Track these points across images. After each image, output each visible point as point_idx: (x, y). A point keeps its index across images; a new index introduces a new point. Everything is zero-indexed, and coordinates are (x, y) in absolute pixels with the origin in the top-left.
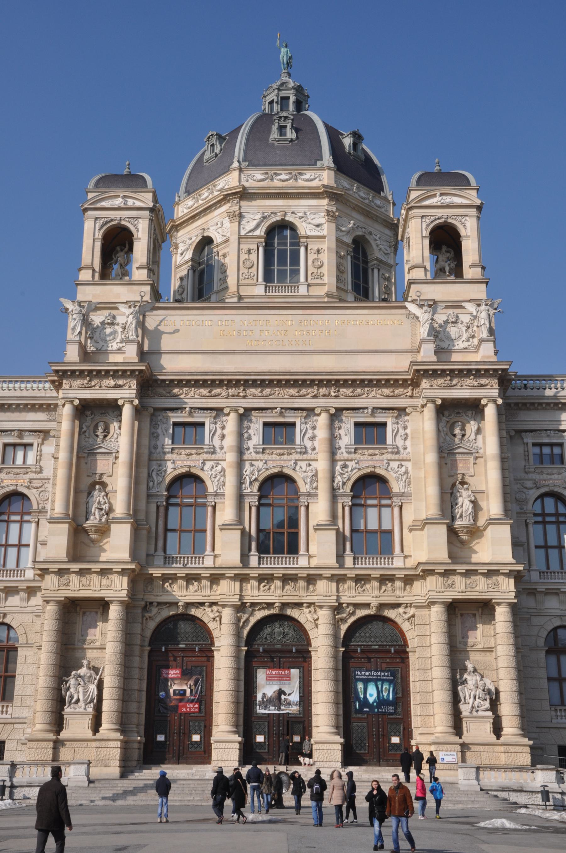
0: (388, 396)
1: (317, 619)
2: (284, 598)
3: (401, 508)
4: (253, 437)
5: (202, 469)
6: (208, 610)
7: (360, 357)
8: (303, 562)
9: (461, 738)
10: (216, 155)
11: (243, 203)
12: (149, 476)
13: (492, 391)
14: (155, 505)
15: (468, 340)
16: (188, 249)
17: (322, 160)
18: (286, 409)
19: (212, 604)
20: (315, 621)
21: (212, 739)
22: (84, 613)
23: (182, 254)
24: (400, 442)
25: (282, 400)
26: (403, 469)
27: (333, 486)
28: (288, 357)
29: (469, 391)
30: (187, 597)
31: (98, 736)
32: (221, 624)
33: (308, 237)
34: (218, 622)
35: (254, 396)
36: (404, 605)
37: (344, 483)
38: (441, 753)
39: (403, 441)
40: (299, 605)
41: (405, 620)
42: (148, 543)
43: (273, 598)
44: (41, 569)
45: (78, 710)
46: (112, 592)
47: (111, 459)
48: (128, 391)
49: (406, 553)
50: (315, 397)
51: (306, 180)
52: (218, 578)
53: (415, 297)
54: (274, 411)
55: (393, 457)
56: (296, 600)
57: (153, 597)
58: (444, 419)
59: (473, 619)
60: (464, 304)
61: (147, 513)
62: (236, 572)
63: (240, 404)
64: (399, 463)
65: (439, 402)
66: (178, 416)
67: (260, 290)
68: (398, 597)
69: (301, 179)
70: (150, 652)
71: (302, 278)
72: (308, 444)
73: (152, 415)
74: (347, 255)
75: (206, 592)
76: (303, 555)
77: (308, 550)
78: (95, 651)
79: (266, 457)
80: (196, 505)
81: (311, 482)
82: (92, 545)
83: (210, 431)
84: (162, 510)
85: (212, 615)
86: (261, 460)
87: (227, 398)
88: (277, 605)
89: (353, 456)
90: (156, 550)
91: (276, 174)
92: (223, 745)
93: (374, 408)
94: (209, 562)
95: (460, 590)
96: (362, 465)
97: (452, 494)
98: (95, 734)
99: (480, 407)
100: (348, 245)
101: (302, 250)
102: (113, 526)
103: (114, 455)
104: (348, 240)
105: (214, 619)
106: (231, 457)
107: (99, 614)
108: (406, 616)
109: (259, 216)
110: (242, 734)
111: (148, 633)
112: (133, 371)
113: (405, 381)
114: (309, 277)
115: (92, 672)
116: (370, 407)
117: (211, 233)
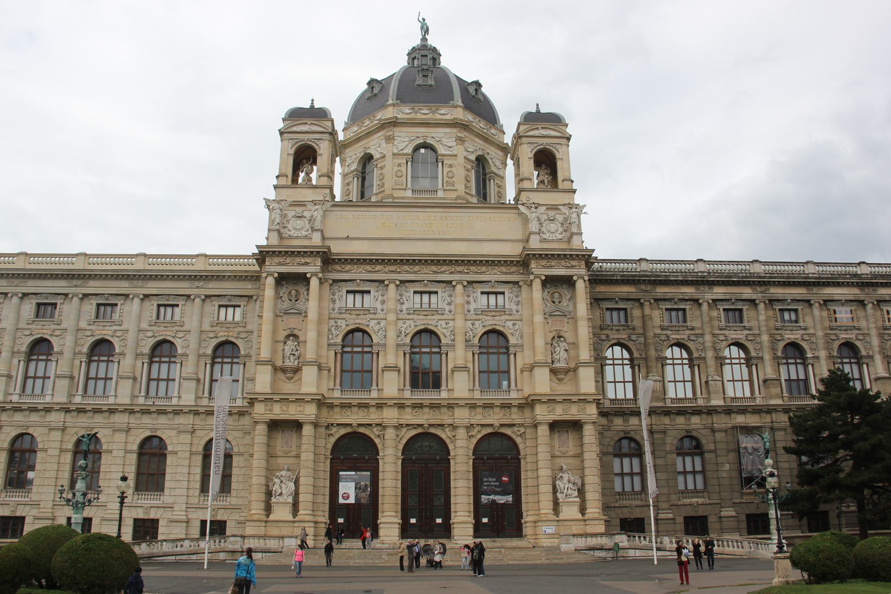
1: (455, 436)
3: (515, 354)
4: (406, 302)
5: (368, 325)
7: (485, 244)
8: (444, 394)
9: (558, 517)
10: (375, 95)
11: (396, 129)
12: (329, 330)
15: (561, 233)
16: (353, 162)
17: (453, 100)
18: (431, 281)
19: (377, 425)
21: (379, 521)
22: (283, 431)
23: (348, 166)
24: (514, 307)
26: (517, 327)
27: (466, 339)
28: (433, 243)
29: (565, 270)
30: (359, 420)
31: (297, 518)
33: (443, 155)
35: (407, 272)
36: (518, 425)
38: (543, 527)
40: (442, 425)
41: (518, 436)
42: (328, 380)
43: (422, 420)
44: (251, 399)
45: (281, 500)
46: (304, 416)
47: (301, 318)
48: (314, 267)
49: (519, 388)
50: (452, 273)
53: (525, 201)
54: (423, 283)
55: (509, 317)
56: (439, 422)
57: (333, 420)
58: (546, 290)
59: (566, 434)
60: (560, 207)
61: (327, 358)
62: (396, 402)
63: (397, 278)
64: (514, 322)
65: (543, 278)
66: (351, 286)
67: (409, 193)
68: (514, 419)
69: (439, 114)
70: (331, 459)
71: (440, 186)
72: (447, 308)
73: (331, 285)
75: (373, 416)
76: (443, 390)
77: (447, 386)
78: (291, 458)
79: (415, 317)
80: (363, 352)
82: (288, 381)
83: (375, 297)
84: (339, 356)
85: (377, 433)
86: (413, 320)
87: (386, 273)
88: (425, 426)
89: (480, 317)
91: (419, 109)
92: (386, 526)
93: (495, 281)
94: (374, 394)
95: (558, 414)
96: (487, 323)
97: (552, 344)
98: (294, 518)
99: (572, 282)
100: (472, 161)
101: (440, 164)
102: (304, 368)
103: (303, 314)
104: (473, 157)
105: (379, 436)
106: (392, 317)
107: (294, 432)
108: (519, 433)
109: (407, 139)
110: (400, 518)
111: (330, 446)
112: (318, 252)
113: (518, 262)
114: (445, 185)
117: (371, 151)
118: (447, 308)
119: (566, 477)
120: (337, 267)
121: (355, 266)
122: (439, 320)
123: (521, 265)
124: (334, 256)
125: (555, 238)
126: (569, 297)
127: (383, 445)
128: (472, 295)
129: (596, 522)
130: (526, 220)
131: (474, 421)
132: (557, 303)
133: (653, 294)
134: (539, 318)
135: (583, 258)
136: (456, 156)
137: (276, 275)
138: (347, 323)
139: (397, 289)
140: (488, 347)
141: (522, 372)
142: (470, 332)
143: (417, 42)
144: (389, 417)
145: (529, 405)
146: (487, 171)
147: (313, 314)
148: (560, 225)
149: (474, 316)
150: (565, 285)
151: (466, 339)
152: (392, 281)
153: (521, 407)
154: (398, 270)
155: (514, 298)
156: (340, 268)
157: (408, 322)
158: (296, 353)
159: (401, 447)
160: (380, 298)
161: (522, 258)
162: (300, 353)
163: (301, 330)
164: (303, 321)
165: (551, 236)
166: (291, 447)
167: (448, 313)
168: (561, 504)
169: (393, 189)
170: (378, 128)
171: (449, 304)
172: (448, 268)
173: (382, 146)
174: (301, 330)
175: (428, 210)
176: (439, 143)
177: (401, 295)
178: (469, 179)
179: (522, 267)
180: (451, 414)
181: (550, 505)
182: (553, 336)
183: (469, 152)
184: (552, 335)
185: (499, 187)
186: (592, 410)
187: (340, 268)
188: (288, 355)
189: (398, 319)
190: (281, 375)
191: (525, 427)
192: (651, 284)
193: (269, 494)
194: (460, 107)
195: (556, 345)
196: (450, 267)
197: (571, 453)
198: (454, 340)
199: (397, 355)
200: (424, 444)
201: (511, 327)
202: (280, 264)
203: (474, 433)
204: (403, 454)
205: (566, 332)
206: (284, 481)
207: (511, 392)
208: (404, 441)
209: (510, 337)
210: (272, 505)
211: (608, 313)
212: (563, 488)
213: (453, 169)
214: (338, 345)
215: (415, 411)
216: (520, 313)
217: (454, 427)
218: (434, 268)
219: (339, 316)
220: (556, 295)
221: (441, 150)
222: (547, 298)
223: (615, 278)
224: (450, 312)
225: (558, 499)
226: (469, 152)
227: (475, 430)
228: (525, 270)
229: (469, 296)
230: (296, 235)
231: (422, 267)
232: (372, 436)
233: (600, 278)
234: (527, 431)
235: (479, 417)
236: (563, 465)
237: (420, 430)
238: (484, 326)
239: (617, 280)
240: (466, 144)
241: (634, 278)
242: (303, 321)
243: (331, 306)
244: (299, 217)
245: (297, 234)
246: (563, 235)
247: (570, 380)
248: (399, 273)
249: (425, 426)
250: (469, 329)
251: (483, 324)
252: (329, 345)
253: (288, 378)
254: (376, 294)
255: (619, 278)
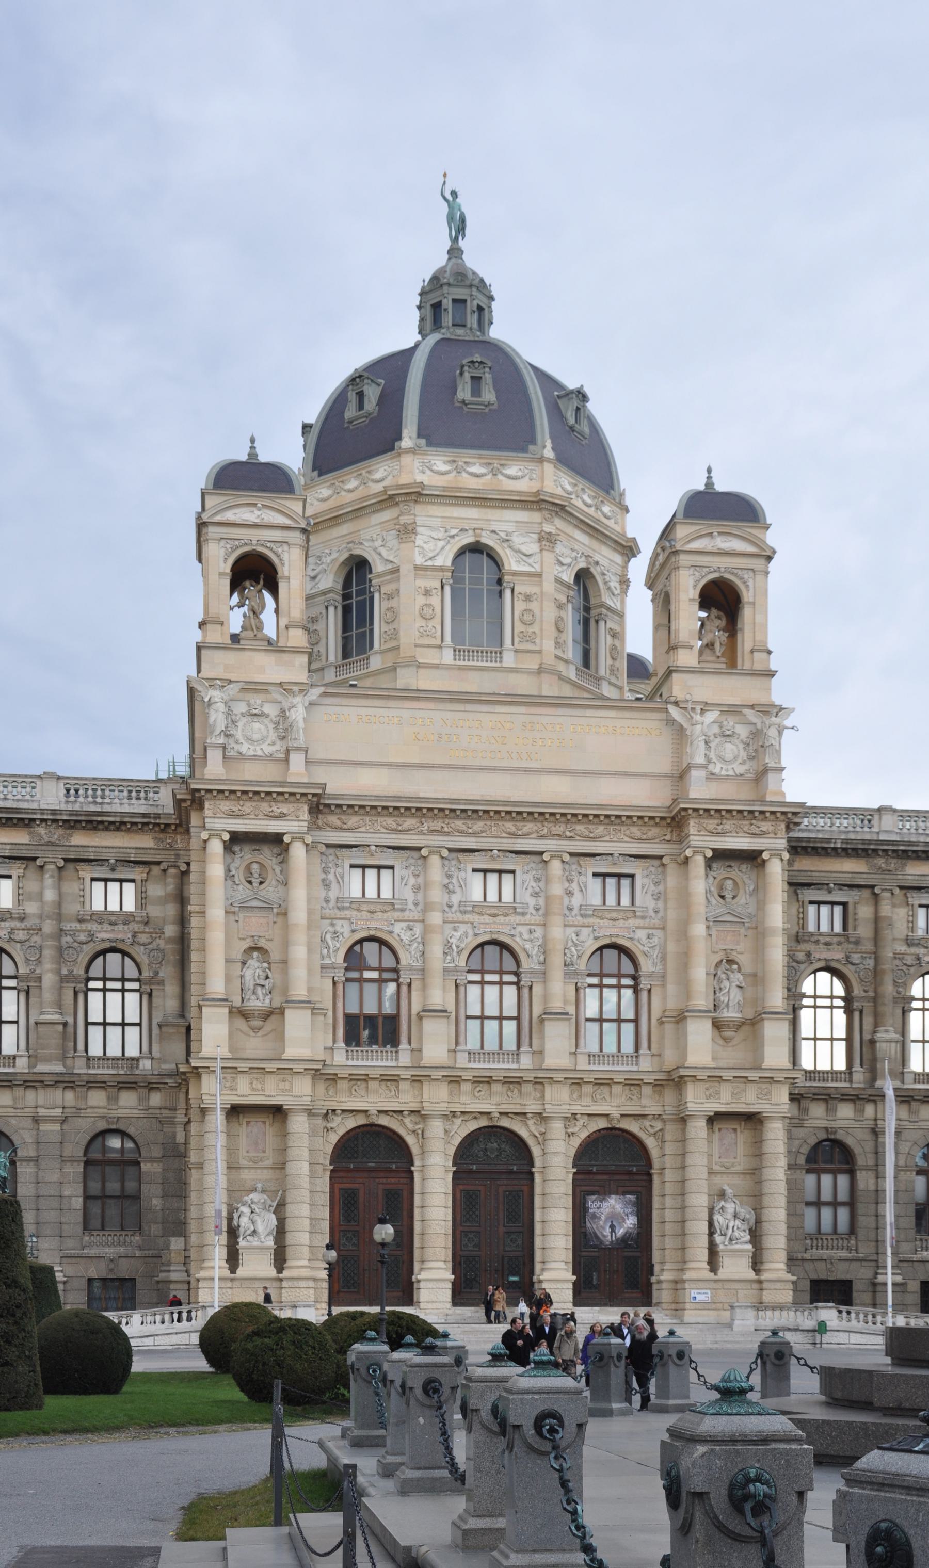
0: (640, 840)
2: (504, 1106)
3: (649, 991)
4: (458, 889)
6: (407, 1121)
9: (716, 1274)
11: (419, 509)
13: (777, 841)
14: (331, 981)
15: (743, 763)
20: (541, 1134)
21: (414, 1277)
22: (248, 1123)
25: (499, 840)
26: (655, 940)
30: (379, 1104)
32: (423, 1137)
33: (514, 574)
34: (420, 1136)
36: (651, 1117)
37: (579, 957)
39: (654, 902)
43: (490, 1106)
46: (291, 1099)
50: (542, 837)
51: (509, 477)
52: (420, 1081)
57: (335, 1103)
59: (733, 1135)
62: (445, 1074)
63: (443, 843)
64: (651, 931)
68: (645, 1107)
74: (568, 601)
77: (531, 1046)
78: (265, 1171)
79: (475, 918)
81: (536, 955)
82: (252, 1033)
83: (402, 878)
87: (424, 834)
88: (493, 1115)
89: (591, 920)
90: (334, 1041)
92: (430, 1285)
99: (759, 860)
100: (568, 586)
101: (507, 594)
103: (275, 910)
107: (268, 1123)
108: (652, 1131)
111: (329, 1149)
113: (662, 818)
115: (266, 1197)
116: (616, 855)
118: (532, 902)
119: (730, 1207)
120: (333, 819)
121: (367, 818)
122: (517, 924)
123: (669, 825)
124: (329, 798)
125: (731, 773)
126: (752, 888)
127: (422, 1147)
128: (576, 879)
129: (778, 1285)
130: (680, 734)
131: (577, 1109)
132: (728, 899)
133: (900, 877)
134: (699, 929)
135: (783, 817)
136: (539, 575)
137: (226, 837)
138: (354, 927)
139: (443, 865)
140: (601, 975)
141: (661, 1023)
142: (573, 949)
143: (439, 260)
144: (434, 1100)
145: (671, 1083)
146: (593, 601)
147: (299, 914)
148: (741, 746)
149: (579, 918)
150: (744, 866)
151: (565, 962)
152: (435, 850)
153: (658, 1085)
154: (446, 829)
155: (652, 887)
156: (338, 823)
157: (463, 928)
158: (266, 983)
159: (452, 1151)
160: (412, 881)
161: (671, 812)
162: (274, 984)
163: (271, 940)
164: (275, 922)
165: (724, 767)
166: (264, 1152)
167: (534, 912)
168: (721, 1254)
169: (416, 646)
170: (379, 502)
171: (536, 895)
172: (536, 828)
173: (390, 544)
174: (271, 940)
175: (499, 709)
176: (505, 545)
177: (449, 876)
178: (561, 626)
179: (669, 829)
180: (539, 1095)
181: (704, 1255)
182: (718, 959)
183: (562, 564)
184: (717, 958)
185: (614, 635)
186: (782, 1095)
187: (338, 823)
188: (252, 988)
189: (444, 922)
190: (240, 1023)
191: (664, 1121)
192: (898, 857)
193: (233, 1233)
194: (549, 461)
195: (723, 976)
196: (539, 825)
197: (738, 1168)
198: (544, 963)
199: (444, 989)
200: (490, 1145)
201: (644, 940)
202: (232, 815)
203: (575, 1130)
204: (454, 1164)
205: (742, 953)
206: (257, 1210)
207: (641, 1059)
208: (457, 1141)
209: (642, 959)
210: (240, 1251)
211: (812, 909)
212: (725, 1227)
213: (534, 606)
214: (339, 968)
215: (478, 1089)
216: (661, 914)
217: (541, 1117)
218: (510, 826)
219: (338, 913)
220: (729, 884)
221: (511, 563)
222: (712, 889)
223: (832, 845)
224: (537, 910)
225: (716, 1245)
226: (562, 564)
227: (578, 1123)
228: (674, 834)
229: (570, 881)
230: (251, 753)
231: (488, 823)
232: (402, 1132)
233: (804, 844)
234: (668, 1127)
235: (587, 1101)
236: (726, 1187)
237: (483, 1122)
238: (596, 938)
239: (835, 849)
240: (559, 548)
241: (866, 847)
242: (275, 922)
243: (323, 894)
244: (255, 715)
245: (255, 750)
246: (746, 767)
247: (745, 1040)
248: (447, 834)
249: (493, 1115)
250: (570, 944)
251: (597, 935)
252: (323, 967)
253: (252, 1029)
254: (405, 872)
255: (839, 845)
